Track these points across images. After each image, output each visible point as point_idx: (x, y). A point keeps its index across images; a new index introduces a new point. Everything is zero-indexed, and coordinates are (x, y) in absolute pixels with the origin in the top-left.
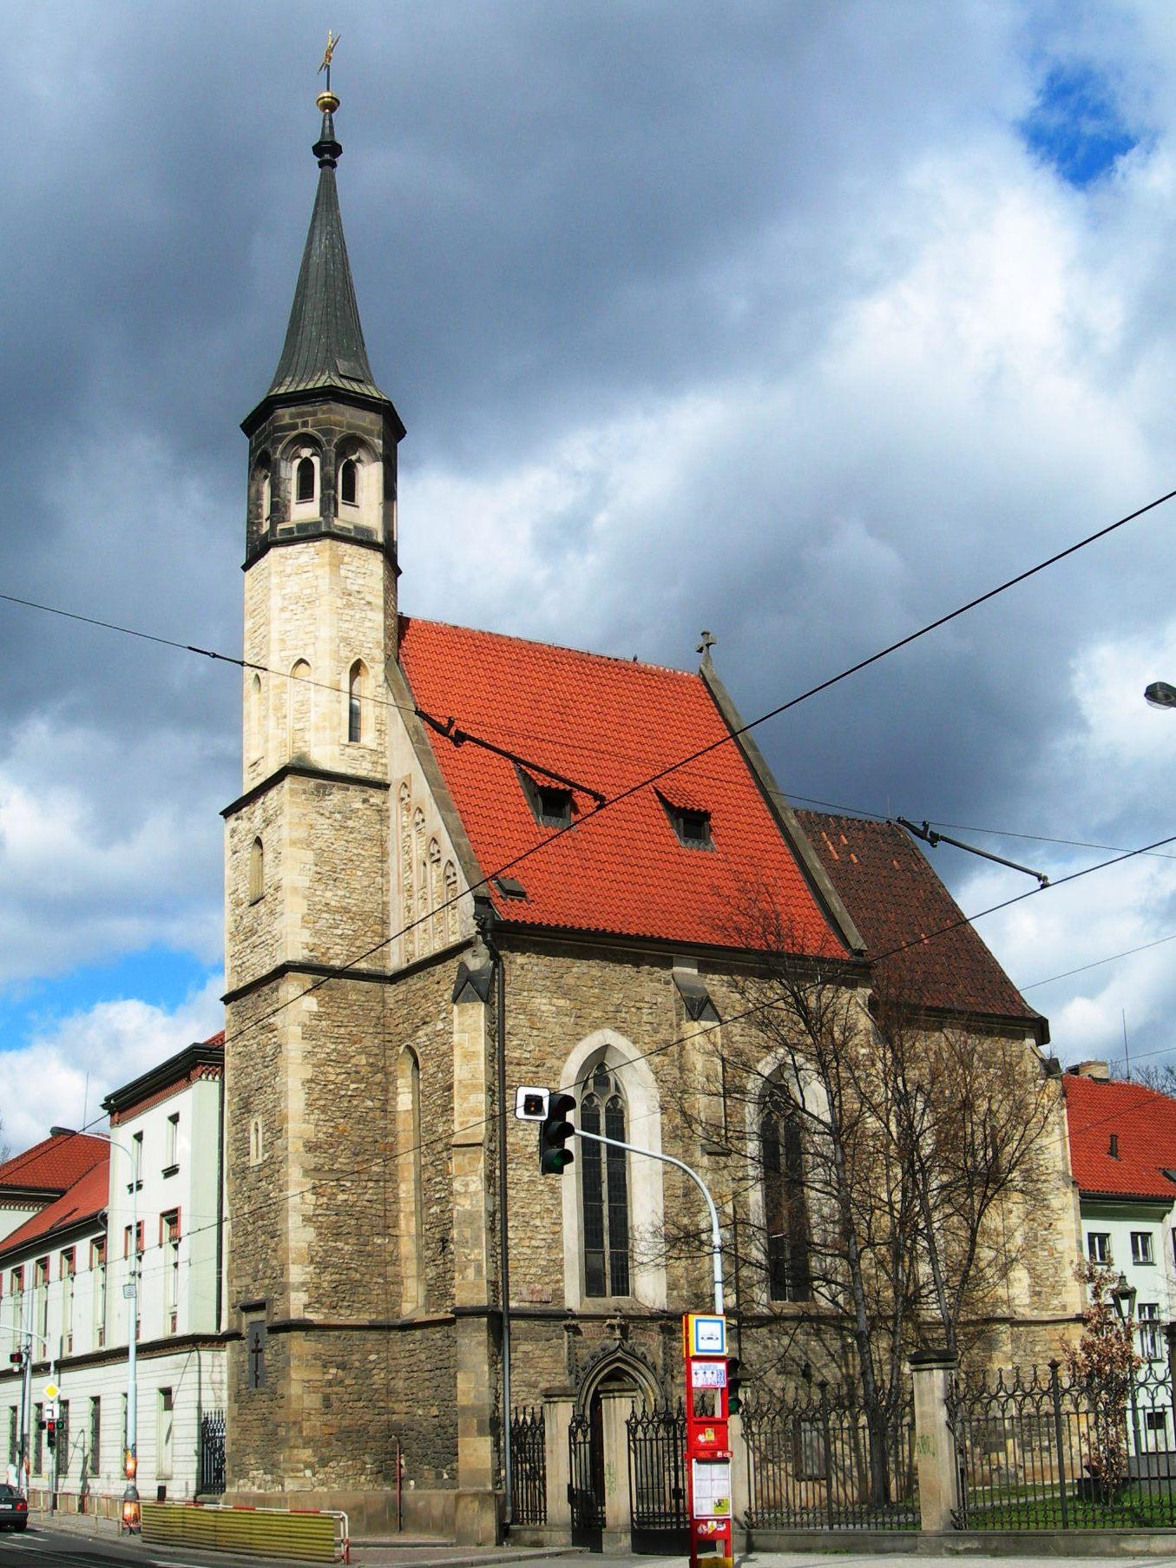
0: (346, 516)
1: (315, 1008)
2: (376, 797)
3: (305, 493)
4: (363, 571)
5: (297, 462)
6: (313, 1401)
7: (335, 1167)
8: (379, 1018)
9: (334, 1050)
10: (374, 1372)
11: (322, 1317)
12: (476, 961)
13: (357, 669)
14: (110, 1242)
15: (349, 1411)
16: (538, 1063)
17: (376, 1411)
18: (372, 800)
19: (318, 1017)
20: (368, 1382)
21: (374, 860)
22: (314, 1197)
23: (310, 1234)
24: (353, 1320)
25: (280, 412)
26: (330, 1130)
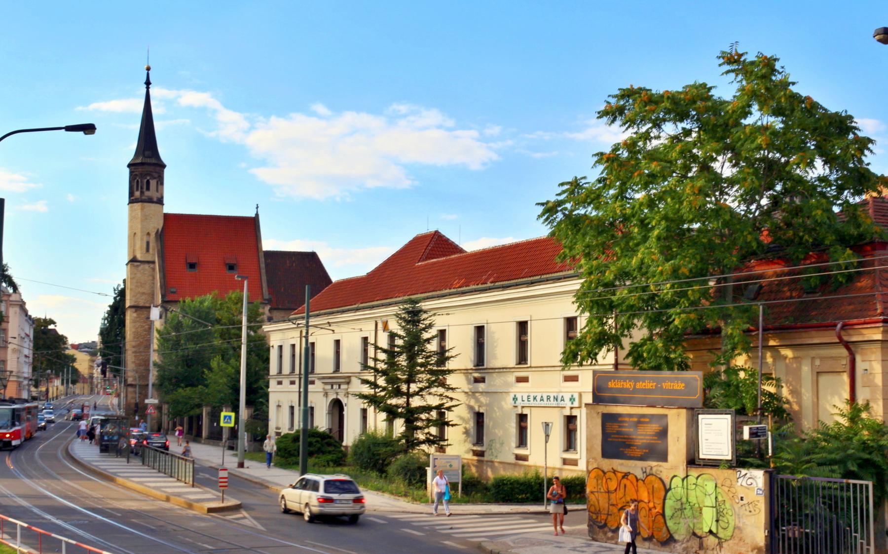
0: (147, 194)
19: (137, 318)
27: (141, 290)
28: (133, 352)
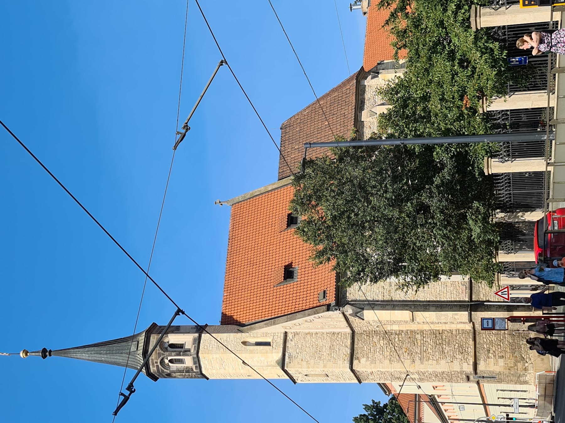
1: (365, 359)
2: (290, 336)
3: (181, 361)
4: (209, 341)
5: (170, 364)
6: (501, 362)
7: (419, 352)
8: (367, 336)
9: (379, 352)
10: (490, 340)
11: (471, 358)
12: (349, 310)
13: (244, 343)
14: (439, 394)
15: (504, 349)
16: (383, 289)
17: (504, 339)
18: (291, 338)
19: (368, 357)
20: (494, 342)
21: (312, 337)
22: (430, 360)
23: (443, 362)
24: (472, 347)
25: (152, 371)
26: (407, 354)
27: (326, 351)
28: (422, 363)
